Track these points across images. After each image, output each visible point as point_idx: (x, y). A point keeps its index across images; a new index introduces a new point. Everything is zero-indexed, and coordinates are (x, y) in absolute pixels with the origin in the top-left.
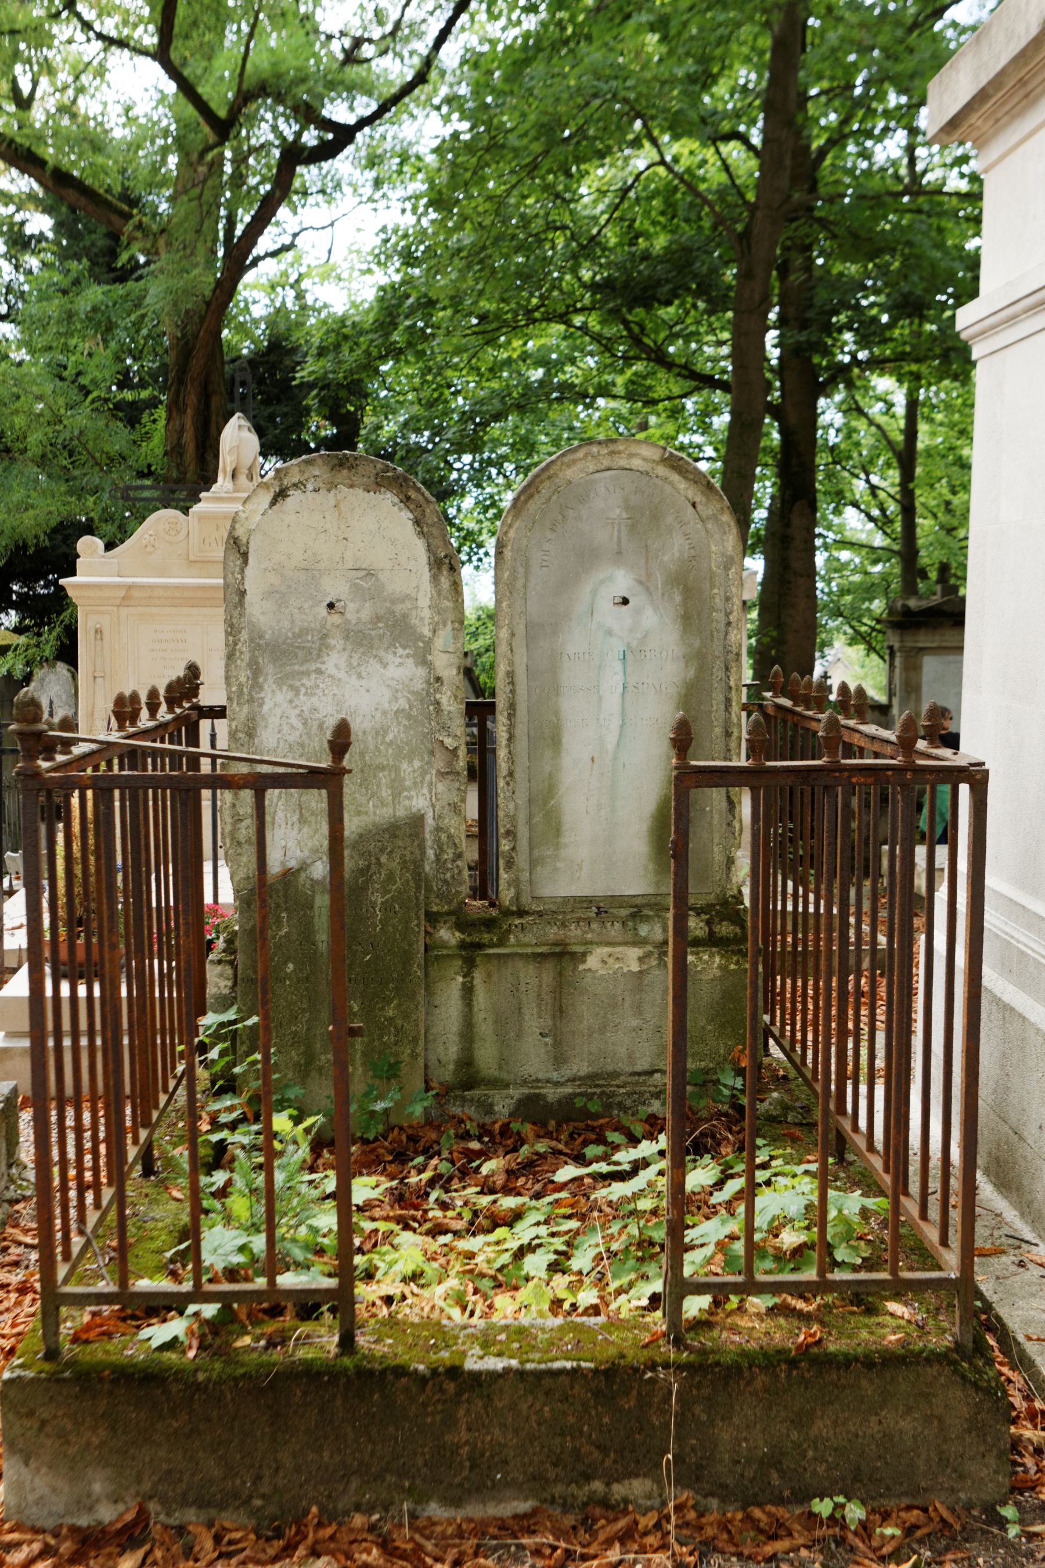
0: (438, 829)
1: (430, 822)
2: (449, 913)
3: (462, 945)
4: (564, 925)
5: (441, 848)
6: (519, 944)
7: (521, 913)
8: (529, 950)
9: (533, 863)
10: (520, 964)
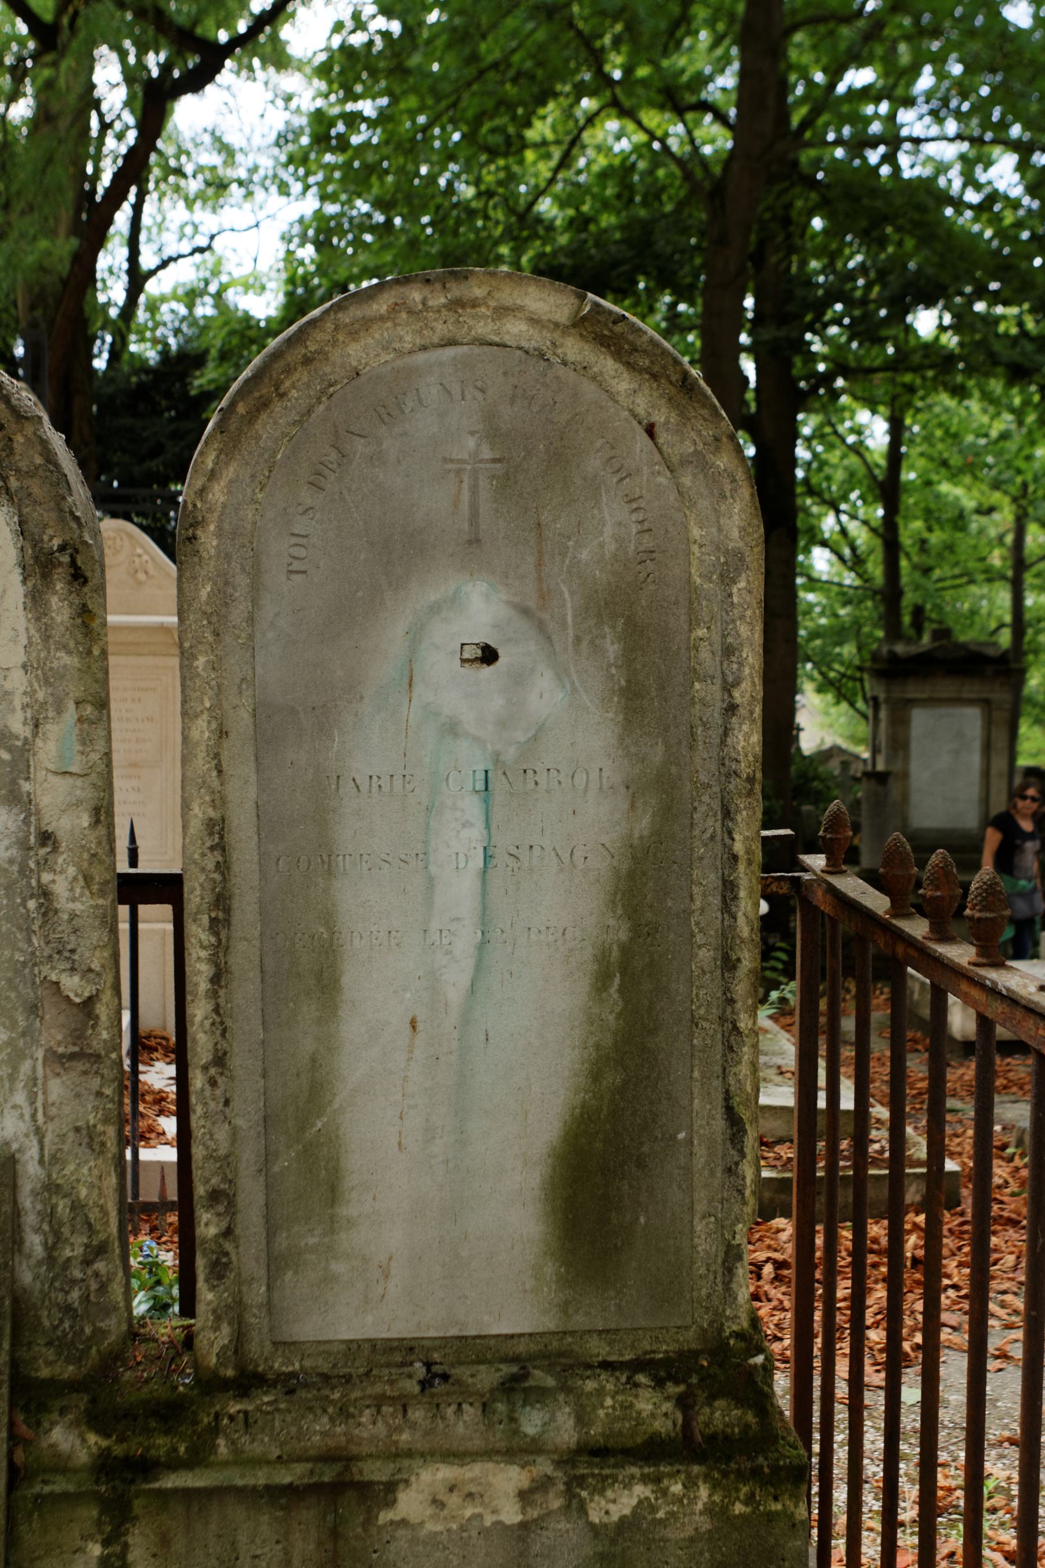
0: (51, 1188)
1: (31, 1169)
2: (74, 1386)
3: (105, 1466)
4: (344, 1413)
5: (57, 1234)
6: (241, 1461)
7: (248, 1381)
8: (260, 1478)
9: (276, 1264)
10: (237, 1513)
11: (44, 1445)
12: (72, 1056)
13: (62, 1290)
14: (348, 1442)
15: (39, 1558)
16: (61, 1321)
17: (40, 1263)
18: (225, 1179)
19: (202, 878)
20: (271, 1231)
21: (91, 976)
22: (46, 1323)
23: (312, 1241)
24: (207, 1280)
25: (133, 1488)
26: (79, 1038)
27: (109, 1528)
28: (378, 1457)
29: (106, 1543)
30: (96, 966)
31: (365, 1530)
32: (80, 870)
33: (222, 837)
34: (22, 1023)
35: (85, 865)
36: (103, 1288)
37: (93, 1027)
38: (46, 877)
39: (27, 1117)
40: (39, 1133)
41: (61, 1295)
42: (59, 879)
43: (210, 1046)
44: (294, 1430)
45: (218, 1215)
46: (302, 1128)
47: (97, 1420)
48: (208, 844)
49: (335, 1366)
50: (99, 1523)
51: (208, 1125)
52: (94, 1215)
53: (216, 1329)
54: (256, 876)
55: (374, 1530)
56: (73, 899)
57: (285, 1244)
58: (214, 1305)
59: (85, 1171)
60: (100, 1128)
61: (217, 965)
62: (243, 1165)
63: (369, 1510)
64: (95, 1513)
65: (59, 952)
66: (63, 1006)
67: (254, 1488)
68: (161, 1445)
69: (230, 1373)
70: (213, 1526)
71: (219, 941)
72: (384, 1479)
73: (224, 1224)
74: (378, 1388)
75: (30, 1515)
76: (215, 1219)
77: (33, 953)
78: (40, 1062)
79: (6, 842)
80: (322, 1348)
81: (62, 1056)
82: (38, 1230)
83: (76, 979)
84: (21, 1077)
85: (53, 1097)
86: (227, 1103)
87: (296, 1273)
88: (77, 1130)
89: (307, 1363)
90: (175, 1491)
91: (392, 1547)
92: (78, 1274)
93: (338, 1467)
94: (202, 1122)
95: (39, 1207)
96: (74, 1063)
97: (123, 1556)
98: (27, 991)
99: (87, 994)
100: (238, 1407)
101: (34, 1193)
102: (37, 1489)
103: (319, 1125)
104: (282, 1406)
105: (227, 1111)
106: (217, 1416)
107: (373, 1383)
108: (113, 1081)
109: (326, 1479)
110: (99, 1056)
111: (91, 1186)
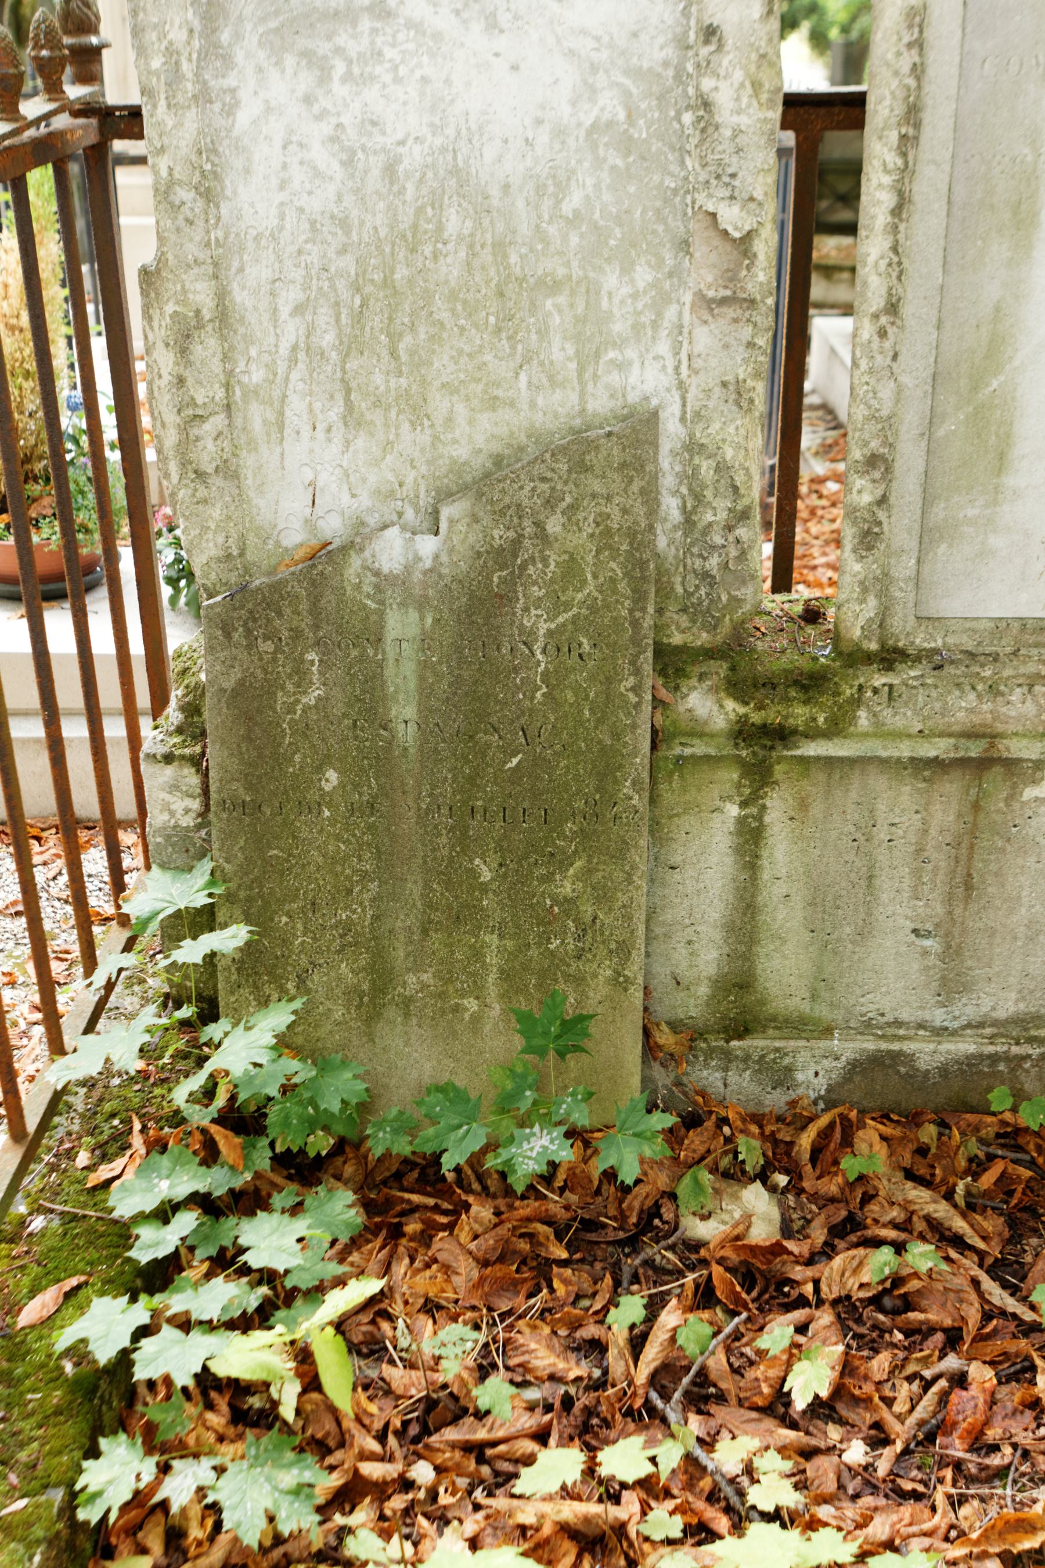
0: (693, 448)
1: (672, 430)
2: (710, 653)
3: (743, 732)
4: (993, 690)
5: (698, 498)
6: (880, 732)
7: (890, 657)
8: (904, 750)
9: (927, 536)
10: (878, 781)
11: (681, 709)
12: (724, 301)
13: (701, 556)
14: (994, 719)
15: (677, 815)
16: (697, 587)
17: (675, 528)
18: (884, 444)
19: (895, 84)
20: (927, 502)
21: (752, 206)
22: (680, 590)
23: (971, 512)
24: (854, 551)
25: (774, 754)
26: (731, 280)
27: (747, 791)
28: (1024, 736)
29: (744, 804)
30: (758, 194)
31: (1008, 805)
32: (747, 75)
33: (921, 32)
34: (669, 262)
35: (753, 68)
36: (742, 556)
37: (748, 268)
38: (707, 84)
39: (670, 370)
40: (682, 387)
41: (698, 562)
42: (723, 85)
43: (884, 291)
44: (937, 706)
45: (874, 481)
46: (975, 389)
47: (738, 687)
48: (906, 39)
49: (979, 644)
50: (739, 786)
51: (872, 381)
52: (739, 479)
53: (862, 601)
54: (954, 83)
55: (1016, 806)
56: (739, 112)
57: (942, 515)
58: (861, 577)
59: (731, 430)
60: (750, 383)
61: (901, 194)
62: (903, 429)
63: (1014, 786)
64: (735, 776)
65: (718, 177)
66: (717, 241)
67: (899, 760)
68: (799, 714)
69: (874, 646)
70: (853, 795)
71: (906, 163)
72: (1034, 757)
73: (879, 492)
74: (1031, 668)
75: (671, 774)
76: (870, 485)
77: (686, 178)
78: (688, 306)
79: (661, 40)
80: (968, 625)
81: (713, 300)
82: (676, 493)
83: (736, 209)
84: (666, 324)
85: (699, 348)
86: (895, 357)
87: (950, 546)
88: (724, 384)
89: (951, 640)
90: (818, 759)
91: (1033, 822)
92: (718, 540)
93: (983, 743)
94: (866, 378)
95: (678, 468)
96: (724, 309)
97: (759, 818)
98: (677, 225)
99: (747, 228)
100: (883, 680)
101: (674, 453)
102: (678, 750)
103: (995, 384)
104: (929, 681)
105: (895, 365)
106: (861, 688)
107: (1025, 663)
108: (767, 330)
109: (973, 755)
110: (753, 301)
111: (738, 447)
